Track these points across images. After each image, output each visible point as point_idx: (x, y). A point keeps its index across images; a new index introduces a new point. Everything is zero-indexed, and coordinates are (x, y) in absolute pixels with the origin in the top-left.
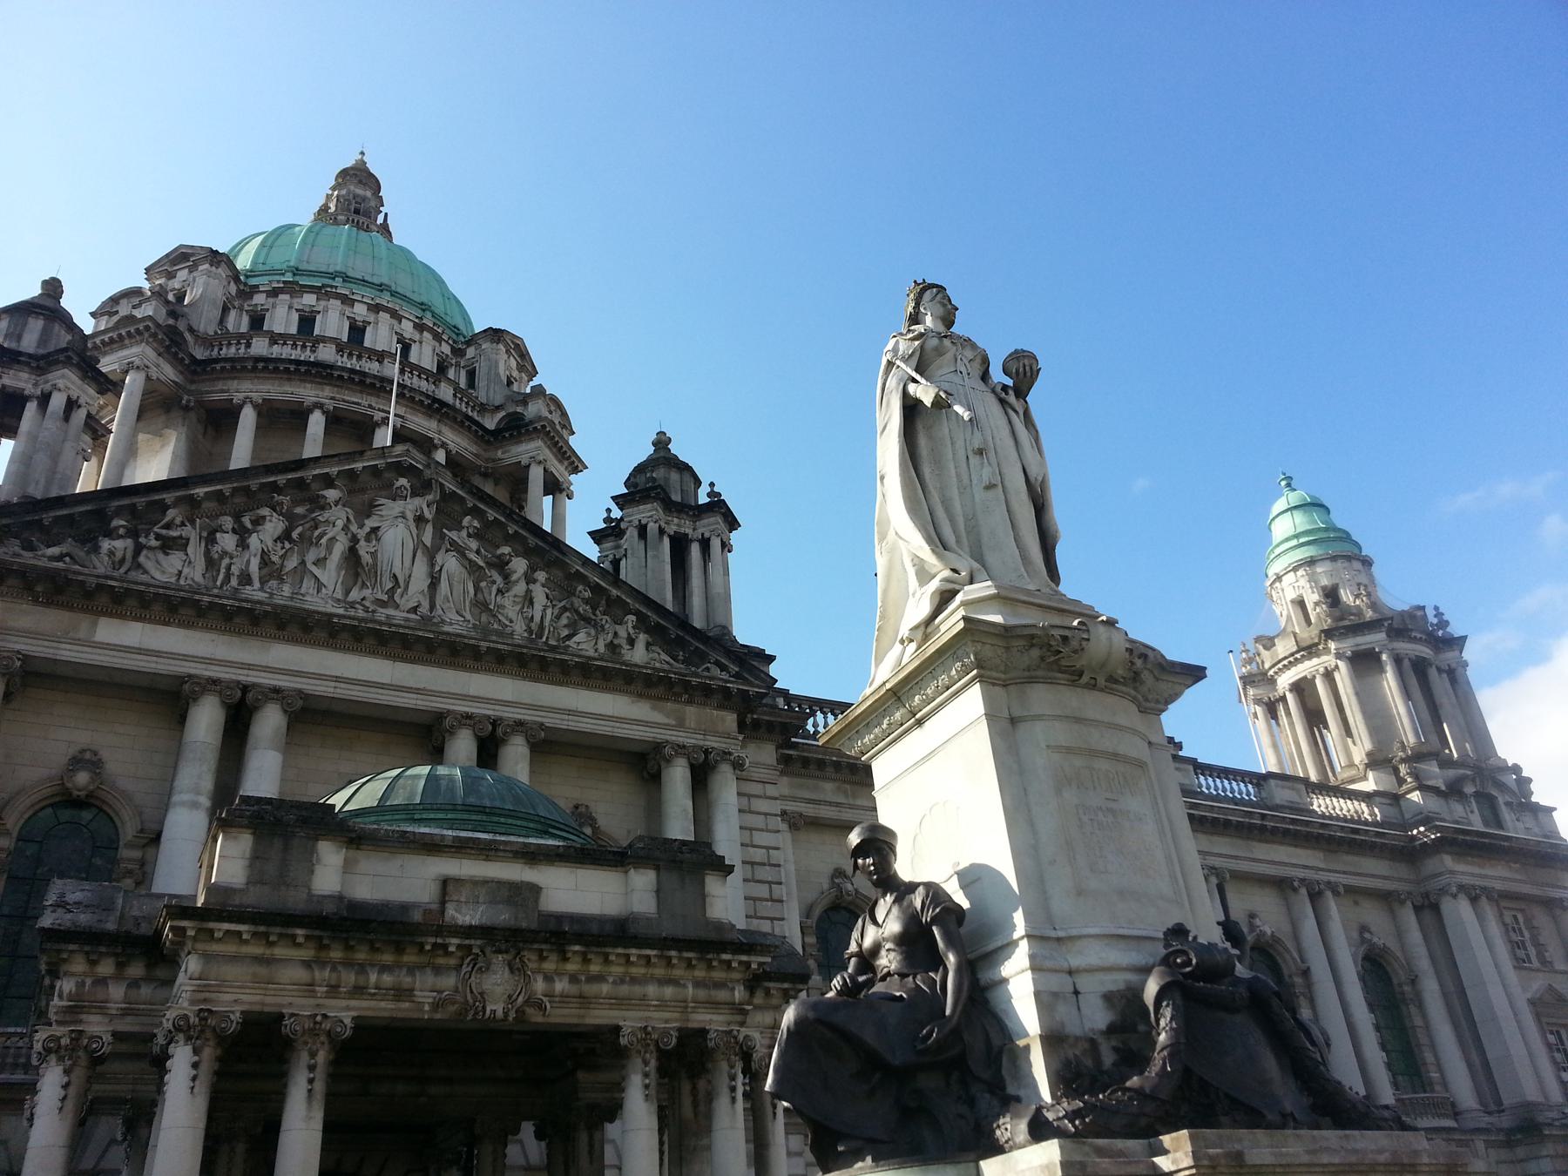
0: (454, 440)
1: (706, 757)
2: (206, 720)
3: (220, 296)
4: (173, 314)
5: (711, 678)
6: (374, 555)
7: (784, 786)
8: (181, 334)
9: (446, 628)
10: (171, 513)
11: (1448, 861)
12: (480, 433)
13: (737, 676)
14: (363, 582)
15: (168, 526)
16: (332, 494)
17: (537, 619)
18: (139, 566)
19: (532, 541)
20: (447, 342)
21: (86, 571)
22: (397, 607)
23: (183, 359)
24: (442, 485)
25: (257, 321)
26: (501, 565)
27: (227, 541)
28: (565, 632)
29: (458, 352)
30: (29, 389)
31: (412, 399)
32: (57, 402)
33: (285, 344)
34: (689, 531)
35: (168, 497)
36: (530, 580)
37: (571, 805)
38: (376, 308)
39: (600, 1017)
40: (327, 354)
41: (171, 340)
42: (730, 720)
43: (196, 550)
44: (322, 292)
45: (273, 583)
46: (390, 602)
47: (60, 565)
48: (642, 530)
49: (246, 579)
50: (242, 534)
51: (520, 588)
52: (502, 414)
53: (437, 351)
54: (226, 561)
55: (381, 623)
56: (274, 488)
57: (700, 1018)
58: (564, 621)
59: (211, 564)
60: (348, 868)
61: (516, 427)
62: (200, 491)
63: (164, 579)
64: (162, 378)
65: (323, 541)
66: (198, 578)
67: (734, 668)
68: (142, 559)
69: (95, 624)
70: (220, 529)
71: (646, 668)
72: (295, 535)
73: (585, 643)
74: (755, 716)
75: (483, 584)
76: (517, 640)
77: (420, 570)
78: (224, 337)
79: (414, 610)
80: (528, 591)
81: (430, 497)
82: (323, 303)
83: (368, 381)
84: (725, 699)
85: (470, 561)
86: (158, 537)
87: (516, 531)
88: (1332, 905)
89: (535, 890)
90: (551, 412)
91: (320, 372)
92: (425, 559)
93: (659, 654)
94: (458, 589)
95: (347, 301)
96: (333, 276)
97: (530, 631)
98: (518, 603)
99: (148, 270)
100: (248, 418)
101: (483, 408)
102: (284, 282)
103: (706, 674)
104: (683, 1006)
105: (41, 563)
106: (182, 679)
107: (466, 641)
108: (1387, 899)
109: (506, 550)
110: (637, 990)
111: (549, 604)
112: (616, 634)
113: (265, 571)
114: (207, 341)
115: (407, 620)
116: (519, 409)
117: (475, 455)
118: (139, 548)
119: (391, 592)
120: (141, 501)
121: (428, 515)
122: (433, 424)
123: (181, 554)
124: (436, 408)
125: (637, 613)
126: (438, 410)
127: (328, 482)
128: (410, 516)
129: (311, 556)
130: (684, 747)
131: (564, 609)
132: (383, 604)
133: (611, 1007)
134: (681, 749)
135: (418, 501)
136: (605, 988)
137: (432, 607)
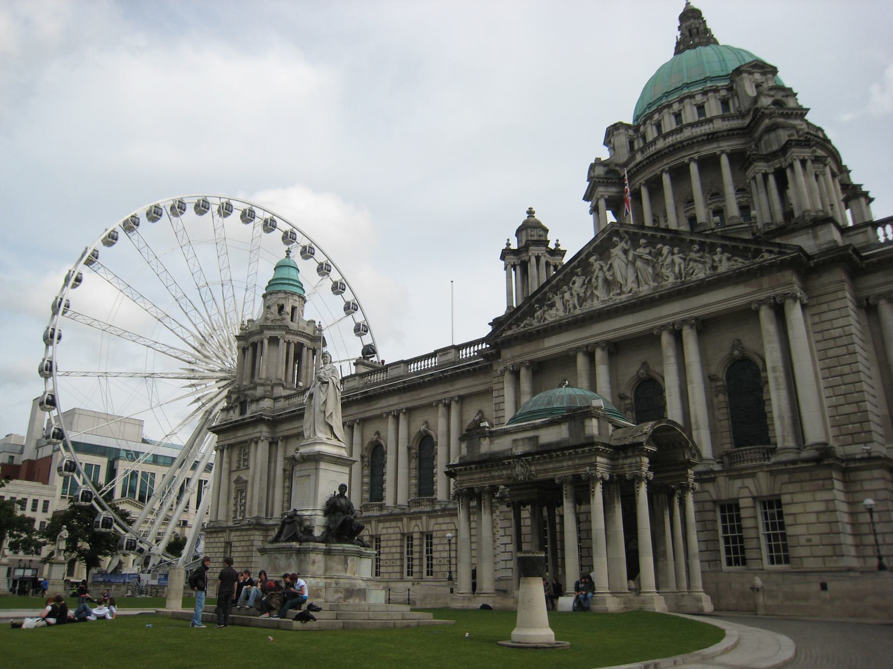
0: (727, 145)
1: (775, 301)
6: (613, 275)
8: (614, 170)
9: (642, 294)
12: (741, 132)
13: (780, 253)
15: (549, 300)
16: (592, 259)
18: (545, 319)
19: (668, 236)
20: (723, 89)
23: (615, 182)
24: (627, 232)
26: (660, 253)
27: (567, 296)
28: (691, 271)
30: (526, 258)
31: (698, 141)
33: (646, 150)
34: (784, 165)
35: (546, 289)
36: (673, 254)
38: (681, 101)
39: (550, 475)
40: (660, 144)
41: (606, 178)
43: (559, 305)
44: (659, 110)
45: (584, 304)
47: (526, 329)
49: (575, 308)
51: (669, 260)
52: (752, 113)
53: (719, 97)
55: (618, 304)
60: (491, 442)
63: (551, 320)
64: (611, 194)
66: (561, 313)
67: (776, 250)
69: (544, 342)
71: (729, 271)
72: (586, 281)
73: (701, 273)
74: (815, 261)
77: (631, 271)
79: (630, 291)
80: (673, 260)
81: (625, 240)
82: (661, 115)
83: (677, 146)
85: (647, 259)
86: (548, 305)
87: (661, 236)
89: (537, 437)
90: (773, 96)
92: (632, 266)
93: (736, 261)
96: (660, 99)
97: (676, 278)
98: (669, 268)
99: (604, 144)
101: (741, 115)
102: (645, 116)
103: (761, 260)
104: (575, 467)
105: (522, 330)
107: (650, 296)
109: (659, 246)
111: (682, 261)
112: (713, 260)
114: (625, 165)
115: (628, 297)
116: (756, 106)
117: (742, 144)
118: (544, 312)
119: (621, 288)
120: (539, 296)
121: (626, 247)
122: (715, 145)
123: (555, 308)
124: (713, 137)
125: (723, 246)
126: (712, 138)
127: (589, 255)
128: (620, 254)
130: (761, 300)
132: (619, 294)
133: (553, 471)
134: (761, 302)
135: (622, 245)
137: (639, 287)
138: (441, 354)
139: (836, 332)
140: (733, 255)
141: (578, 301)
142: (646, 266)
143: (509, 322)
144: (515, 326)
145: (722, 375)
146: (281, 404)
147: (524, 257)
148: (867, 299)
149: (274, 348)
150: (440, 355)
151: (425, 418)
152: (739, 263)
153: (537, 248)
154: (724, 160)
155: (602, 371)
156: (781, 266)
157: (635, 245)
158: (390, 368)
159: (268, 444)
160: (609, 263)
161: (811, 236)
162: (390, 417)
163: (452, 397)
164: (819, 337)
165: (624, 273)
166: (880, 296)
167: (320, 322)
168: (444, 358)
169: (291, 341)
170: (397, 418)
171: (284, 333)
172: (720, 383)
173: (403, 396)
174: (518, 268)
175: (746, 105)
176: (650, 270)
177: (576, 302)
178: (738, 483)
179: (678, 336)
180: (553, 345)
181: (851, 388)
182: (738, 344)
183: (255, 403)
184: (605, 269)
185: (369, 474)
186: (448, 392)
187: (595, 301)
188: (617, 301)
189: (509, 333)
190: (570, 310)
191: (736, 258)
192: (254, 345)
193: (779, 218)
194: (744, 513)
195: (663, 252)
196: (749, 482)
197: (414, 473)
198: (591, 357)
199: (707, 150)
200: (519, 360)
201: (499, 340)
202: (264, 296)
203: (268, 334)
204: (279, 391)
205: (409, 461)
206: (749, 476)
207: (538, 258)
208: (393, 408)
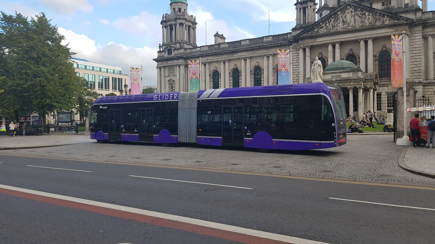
2: (330, 48)
5: (400, 23)
9: (356, 28)
10: (321, 23)
13: (406, 20)
14: (345, 24)
15: (321, 25)
16: (339, 13)
17: (370, 22)
18: (318, 32)
21: (313, 34)
22: (350, 26)
24: (354, 5)
26: (364, 14)
27: (328, 25)
28: (375, 22)
32: (309, 7)
36: (369, 15)
37: (383, 45)
39: (345, 87)
43: (324, 27)
46: (349, 26)
49: (330, 29)
51: (367, 17)
54: (328, 27)
56: (332, 15)
57: (356, 86)
58: (375, 20)
59: (326, 28)
62: (323, 19)
63: (321, 32)
65: (339, 21)
66: (325, 31)
68: (319, 31)
70: (326, 23)
72: (335, 21)
73: (378, 24)
75: (362, 18)
76: (367, 26)
79: (352, 26)
80: (369, 17)
81: (352, 8)
85: (360, 16)
89: (341, 75)
93: (391, 21)
94: (358, 21)
110: (350, 84)
111: (372, 18)
112: (383, 20)
113: (333, 27)
118: (318, 29)
121: (352, 11)
123: (323, 28)
125: (387, 15)
128: (350, 12)
131: (375, 18)
135: (351, 9)
136: (346, 84)
137: (355, 24)
138: (266, 38)
140: (391, 19)
141: (332, 27)
142: (359, 18)
143: (304, 31)
144: (306, 33)
145: (378, 55)
146: (189, 51)
148: (426, 36)
149: (181, 27)
150: (265, 38)
151: (257, 61)
152: (392, 22)
153: (310, 3)
155: (338, 51)
156: (406, 24)
157: (356, 11)
158: (242, 41)
159: (184, 67)
160: (345, 15)
161: (414, 14)
162: (243, 60)
163: (270, 54)
164: (411, 47)
165: (350, 20)
167: (195, 17)
168: (267, 40)
169: (187, 25)
170: (245, 60)
171: (185, 21)
172: (376, 58)
173: (248, 52)
174: (302, 9)
176: (360, 20)
177: (331, 28)
178: (382, 88)
179: (366, 42)
180: (320, 41)
181: (418, 63)
182: (384, 46)
183: (177, 50)
184: (343, 17)
185: (232, 79)
186: (269, 52)
187: (338, 27)
188: (347, 29)
189: (304, 35)
190: (328, 30)
191: (391, 20)
192: (171, 26)
194: (382, 96)
195: (366, 14)
196: (385, 88)
197: (253, 79)
198: (334, 46)
200: (306, 45)
201: (299, 38)
202: (171, 4)
203: (179, 21)
204: (186, 46)
205: (251, 75)
206: (385, 86)
207: (311, 7)
208: (244, 56)
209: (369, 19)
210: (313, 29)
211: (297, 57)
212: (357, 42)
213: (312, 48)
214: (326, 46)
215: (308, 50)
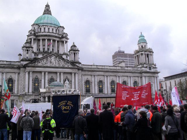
0: (57, 39)
2: (43, 73)
3: (37, 28)
4: (34, 32)
7: (83, 72)
11: (143, 74)
16: (48, 57)
25: (41, 29)
26: (60, 60)
27: (43, 62)
29: (58, 28)
32: (30, 50)
38: (50, 26)
42: (77, 70)
43: (41, 63)
48: (71, 53)
49: (44, 64)
50: (43, 61)
61: (63, 37)
73: (66, 66)
78: (38, 33)
84: (76, 69)
88: (132, 78)
91: (46, 36)
95: (48, 26)
100: (41, 40)
101: (60, 35)
106: (41, 71)
108: (138, 77)
114: (37, 33)
124: (56, 37)
127: (48, 56)
129: (48, 62)
139: (80, 79)
147: (28, 49)
152: (72, 67)
154: (56, 41)
157: (56, 58)
166: (83, 75)
168: (3, 63)
175: (60, 33)
180: (38, 69)
193: (74, 60)
199: (55, 39)
200: (30, 70)
209: (62, 63)
210: (35, 62)
211: (24, 76)
212: (56, 73)
213: (34, 72)
214: (41, 72)
215: (31, 73)
